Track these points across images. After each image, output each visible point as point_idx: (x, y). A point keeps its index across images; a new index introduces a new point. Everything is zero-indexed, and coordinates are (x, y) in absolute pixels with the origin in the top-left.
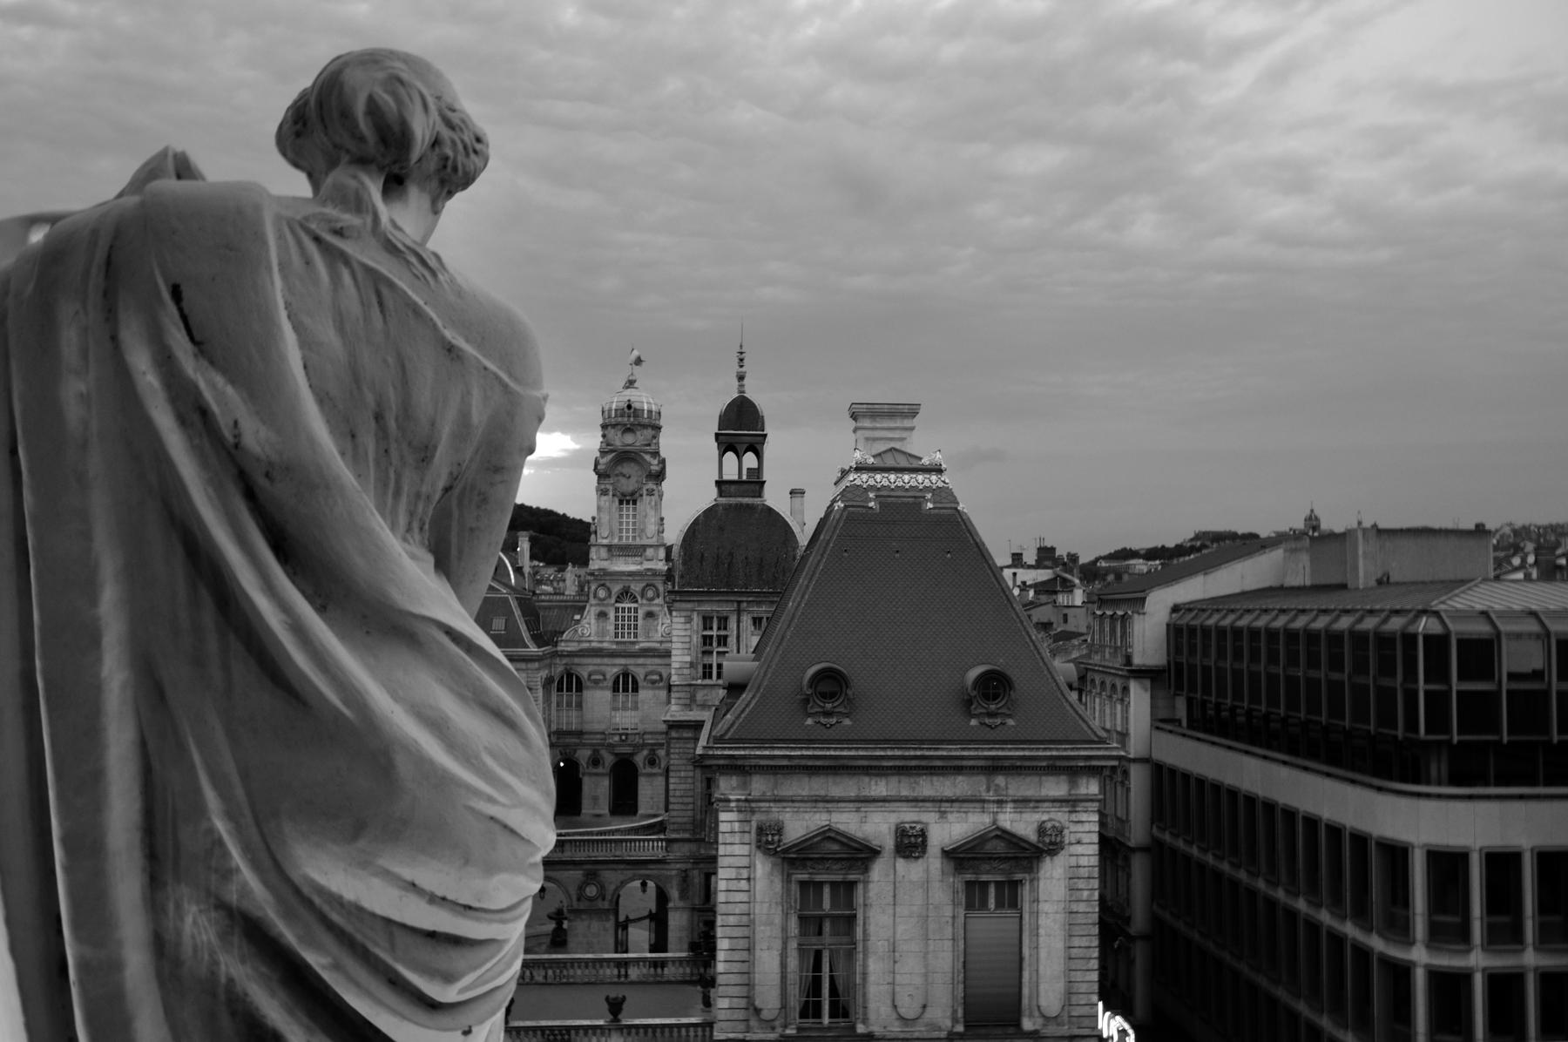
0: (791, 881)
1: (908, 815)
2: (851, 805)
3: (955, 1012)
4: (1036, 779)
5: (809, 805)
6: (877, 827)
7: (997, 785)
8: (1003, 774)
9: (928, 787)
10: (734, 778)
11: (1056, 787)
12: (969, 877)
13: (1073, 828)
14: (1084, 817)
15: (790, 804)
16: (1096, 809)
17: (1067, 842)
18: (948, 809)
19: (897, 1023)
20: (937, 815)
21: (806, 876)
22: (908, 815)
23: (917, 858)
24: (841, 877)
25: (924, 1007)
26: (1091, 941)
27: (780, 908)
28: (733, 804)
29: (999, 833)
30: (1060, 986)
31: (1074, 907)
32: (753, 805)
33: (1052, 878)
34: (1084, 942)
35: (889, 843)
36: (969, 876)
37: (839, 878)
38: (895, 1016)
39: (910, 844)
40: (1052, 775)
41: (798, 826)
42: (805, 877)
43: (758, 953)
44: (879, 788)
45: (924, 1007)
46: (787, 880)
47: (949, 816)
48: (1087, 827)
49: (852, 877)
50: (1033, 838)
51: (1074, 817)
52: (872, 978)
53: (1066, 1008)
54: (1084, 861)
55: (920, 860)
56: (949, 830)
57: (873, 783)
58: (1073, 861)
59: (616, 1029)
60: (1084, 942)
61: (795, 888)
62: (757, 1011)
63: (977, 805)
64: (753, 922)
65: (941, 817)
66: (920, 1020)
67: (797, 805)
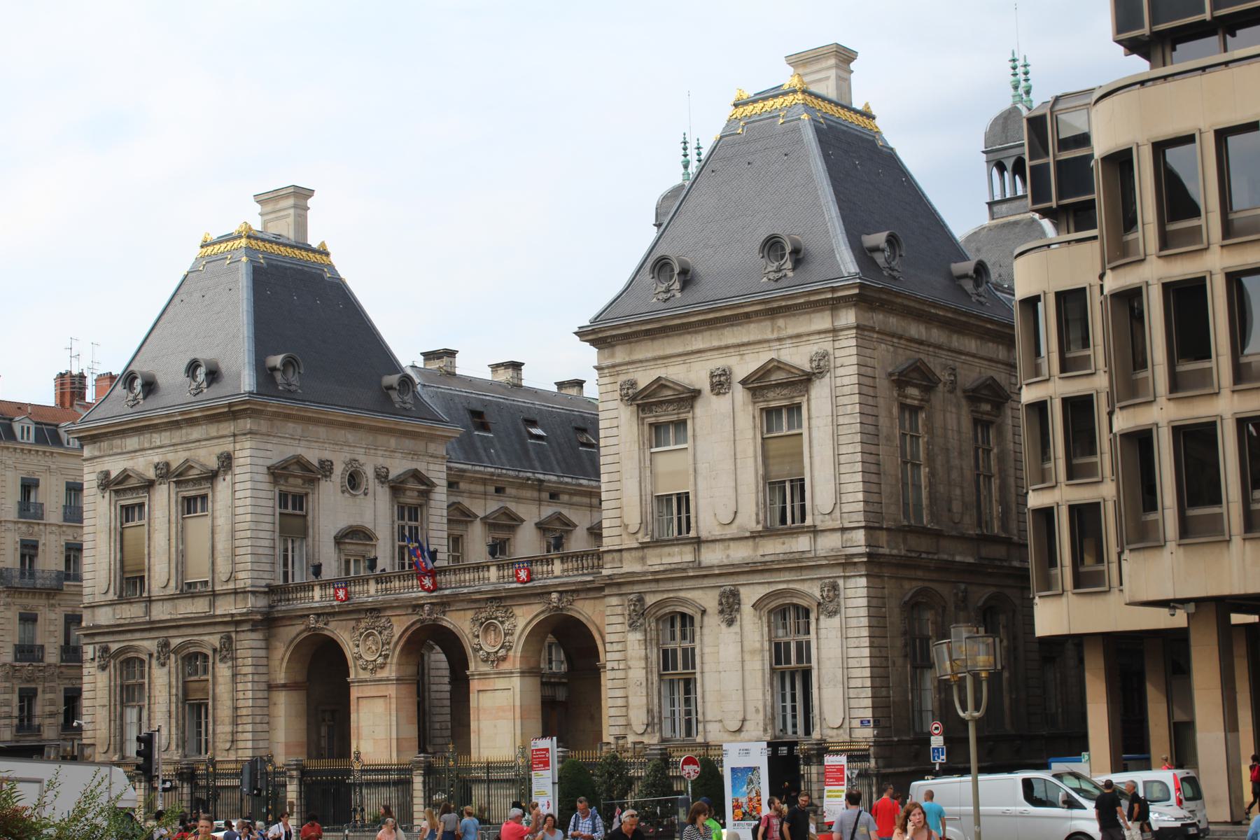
0: (643, 424)
1: (718, 362)
2: (679, 359)
3: (757, 515)
4: (807, 317)
5: (652, 363)
6: (695, 374)
7: (779, 327)
8: (782, 317)
9: (732, 336)
10: (606, 350)
11: (822, 321)
12: (763, 405)
13: (838, 353)
14: (844, 343)
15: (640, 365)
16: (854, 335)
17: (832, 365)
18: (745, 352)
19: (718, 528)
20: (738, 358)
21: (653, 419)
22: (718, 362)
23: (725, 394)
24: (676, 416)
25: (736, 513)
26: (855, 447)
27: (637, 445)
28: (606, 371)
29: (776, 364)
30: (831, 487)
31: (841, 421)
32: (617, 369)
33: (819, 399)
34: (850, 449)
35: (705, 386)
36: (762, 404)
37: (674, 418)
38: (716, 523)
39: (721, 383)
40: (818, 311)
41: (644, 378)
42: (652, 420)
43: (624, 481)
44: (698, 342)
45: (736, 513)
46: (641, 421)
47: (746, 356)
48: (847, 351)
49: (683, 416)
50: (807, 367)
51: (837, 345)
52: (700, 494)
53: (838, 506)
54: (846, 381)
55: (727, 395)
56: (745, 366)
57: (693, 339)
58: (839, 382)
59: (557, 558)
60: (850, 449)
61: (646, 428)
62: (626, 526)
63: (766, 345)
64: (620, 458)
65: (742, 359)
66: (734, 526)
67: (644, 364)
